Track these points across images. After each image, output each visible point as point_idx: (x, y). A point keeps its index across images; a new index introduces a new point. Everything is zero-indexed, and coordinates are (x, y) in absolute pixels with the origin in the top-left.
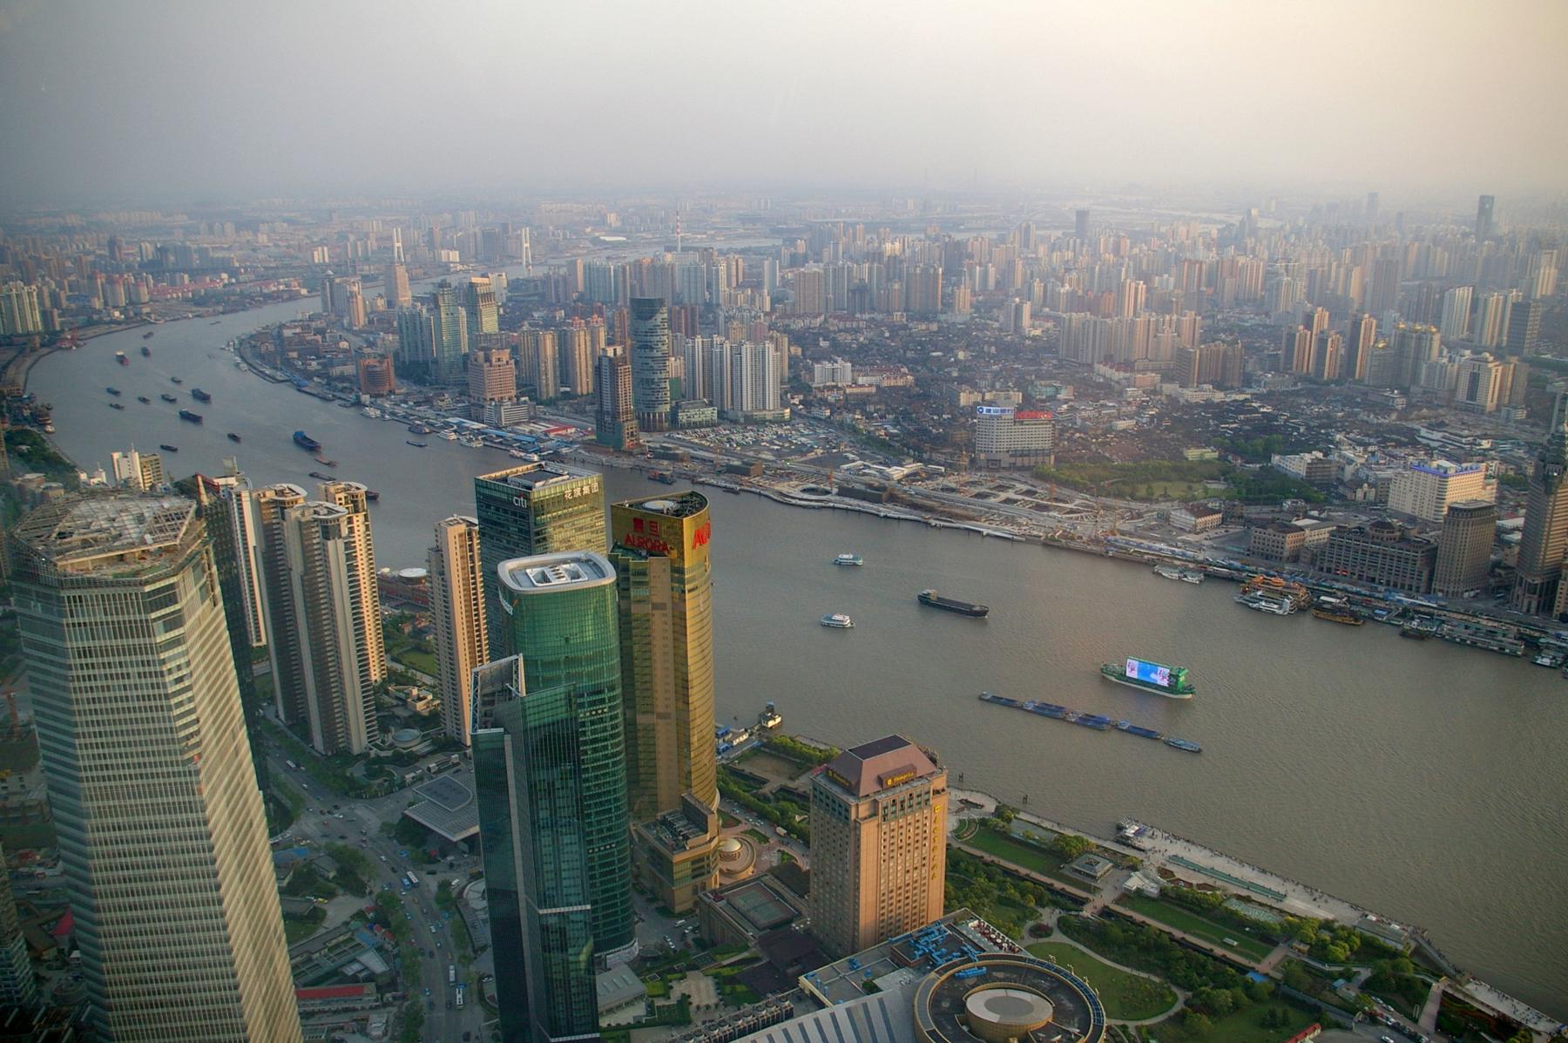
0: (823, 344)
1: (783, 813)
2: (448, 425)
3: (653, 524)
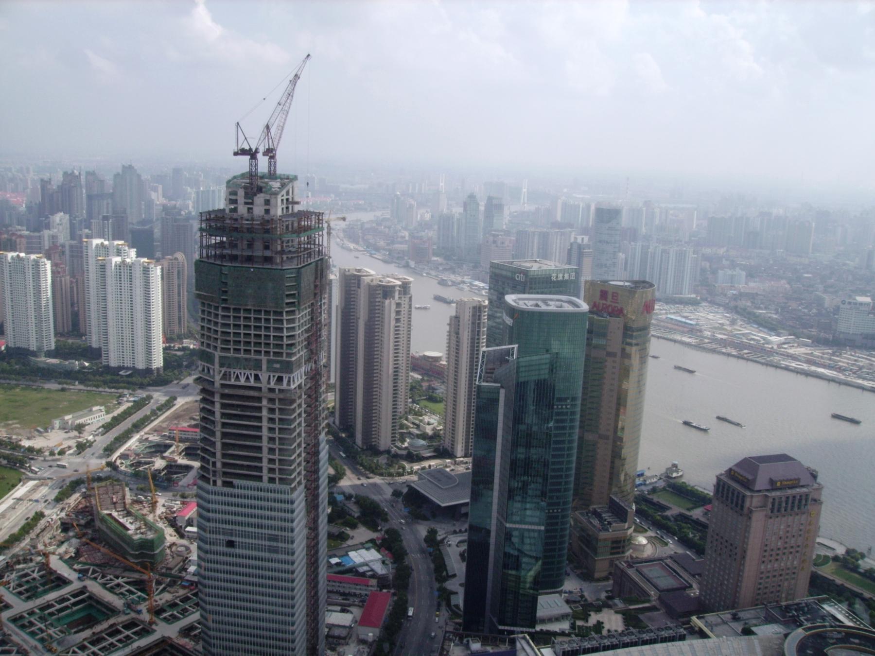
0: (724, 262)
1: (680, 528)
2: (463, 282)
3: (615, 295)
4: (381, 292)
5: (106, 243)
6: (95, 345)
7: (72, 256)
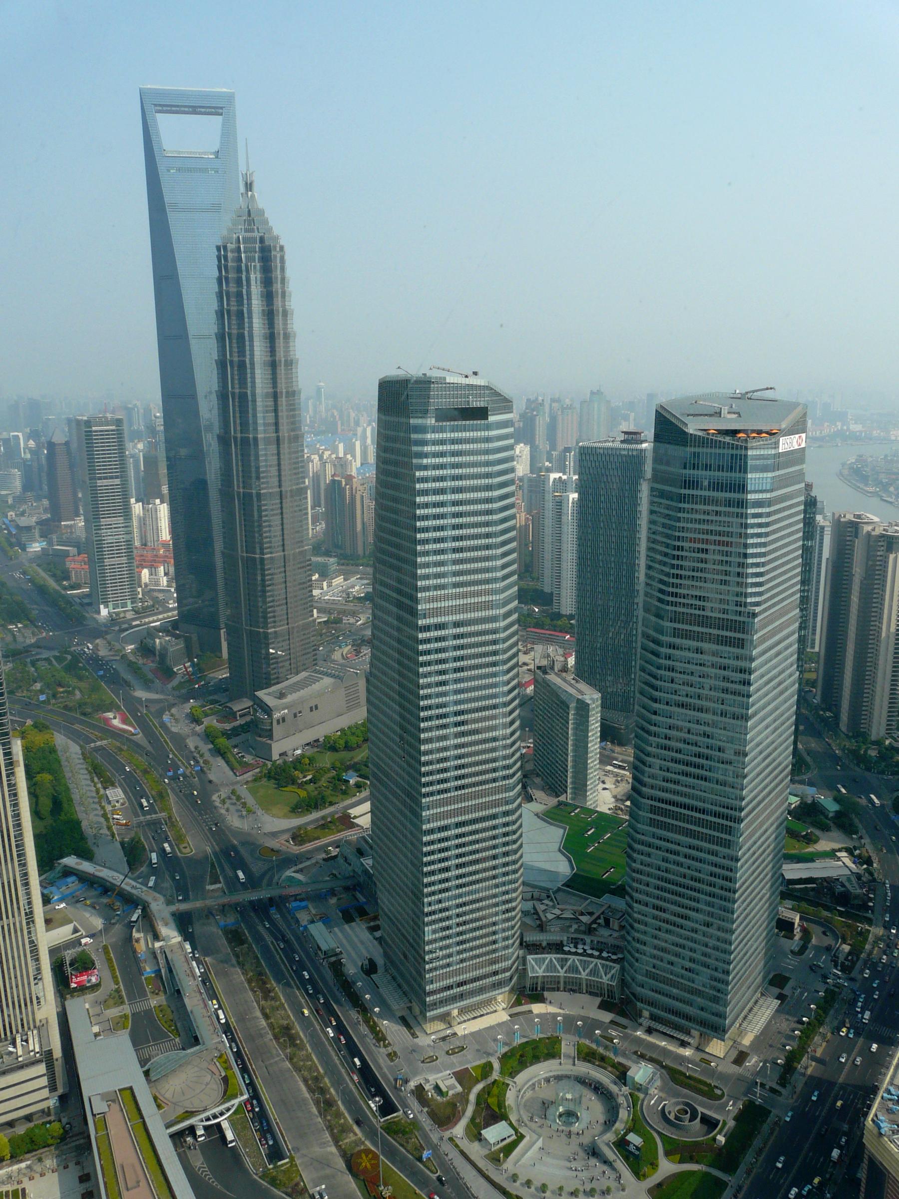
4: (884, 544)
6: (547, 589)
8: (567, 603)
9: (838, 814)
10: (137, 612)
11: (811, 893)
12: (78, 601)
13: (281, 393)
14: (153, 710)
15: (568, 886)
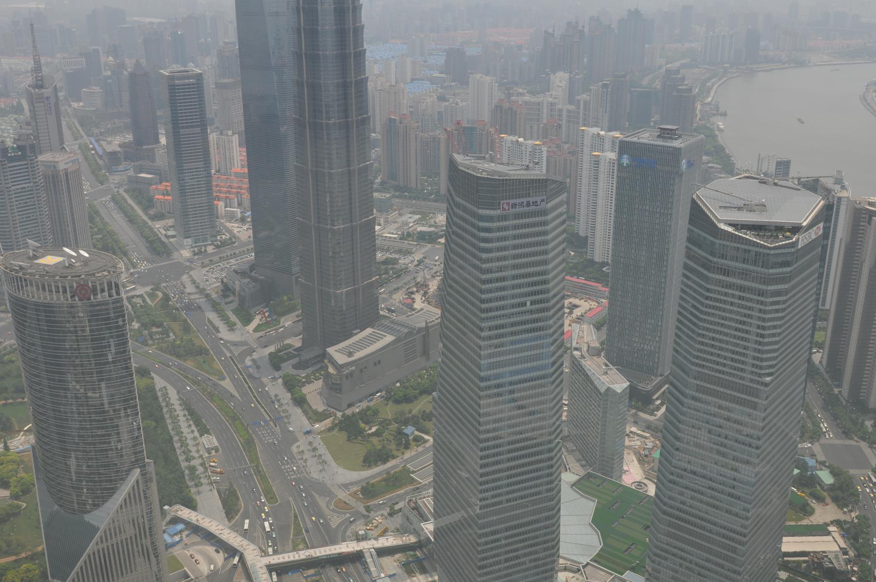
5: (602, 133)
6: (582, 233)
7: (569, 122)
8: (601, 248)
9: (832, 488)
10: (217, 247)
11: (804, 565)
12: (163, 232)
13: (351, 82)
14: (236, 354)
15: (595, 561)
